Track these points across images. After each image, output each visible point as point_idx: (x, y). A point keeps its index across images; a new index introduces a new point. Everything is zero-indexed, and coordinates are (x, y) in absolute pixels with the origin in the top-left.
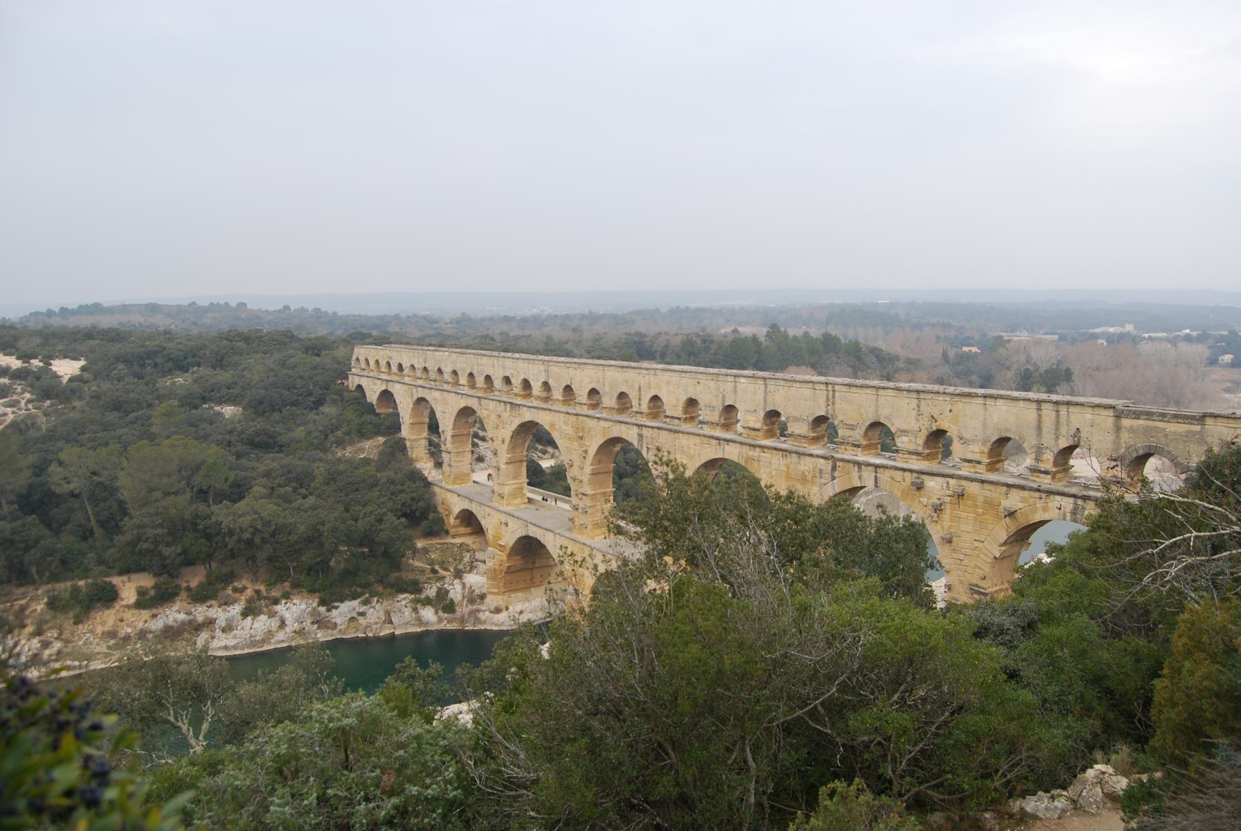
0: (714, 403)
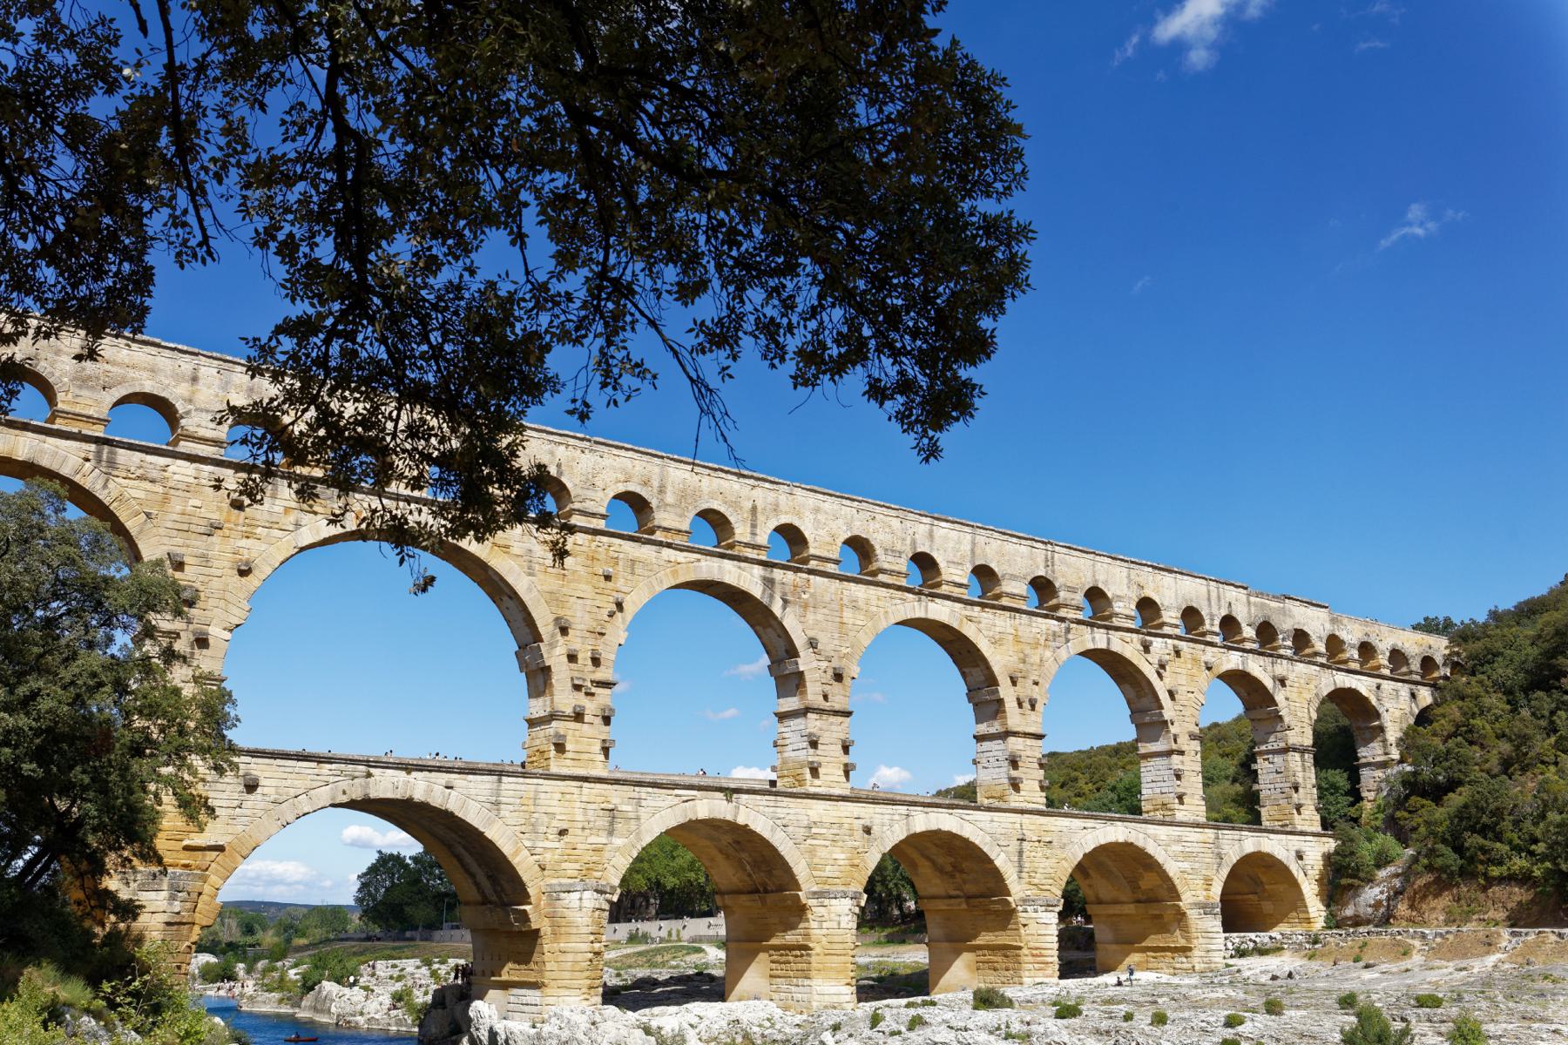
0: (898, 547)
